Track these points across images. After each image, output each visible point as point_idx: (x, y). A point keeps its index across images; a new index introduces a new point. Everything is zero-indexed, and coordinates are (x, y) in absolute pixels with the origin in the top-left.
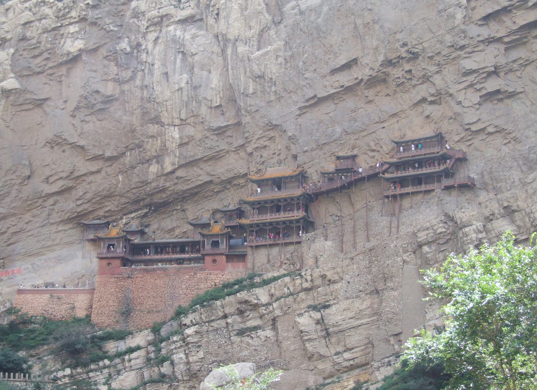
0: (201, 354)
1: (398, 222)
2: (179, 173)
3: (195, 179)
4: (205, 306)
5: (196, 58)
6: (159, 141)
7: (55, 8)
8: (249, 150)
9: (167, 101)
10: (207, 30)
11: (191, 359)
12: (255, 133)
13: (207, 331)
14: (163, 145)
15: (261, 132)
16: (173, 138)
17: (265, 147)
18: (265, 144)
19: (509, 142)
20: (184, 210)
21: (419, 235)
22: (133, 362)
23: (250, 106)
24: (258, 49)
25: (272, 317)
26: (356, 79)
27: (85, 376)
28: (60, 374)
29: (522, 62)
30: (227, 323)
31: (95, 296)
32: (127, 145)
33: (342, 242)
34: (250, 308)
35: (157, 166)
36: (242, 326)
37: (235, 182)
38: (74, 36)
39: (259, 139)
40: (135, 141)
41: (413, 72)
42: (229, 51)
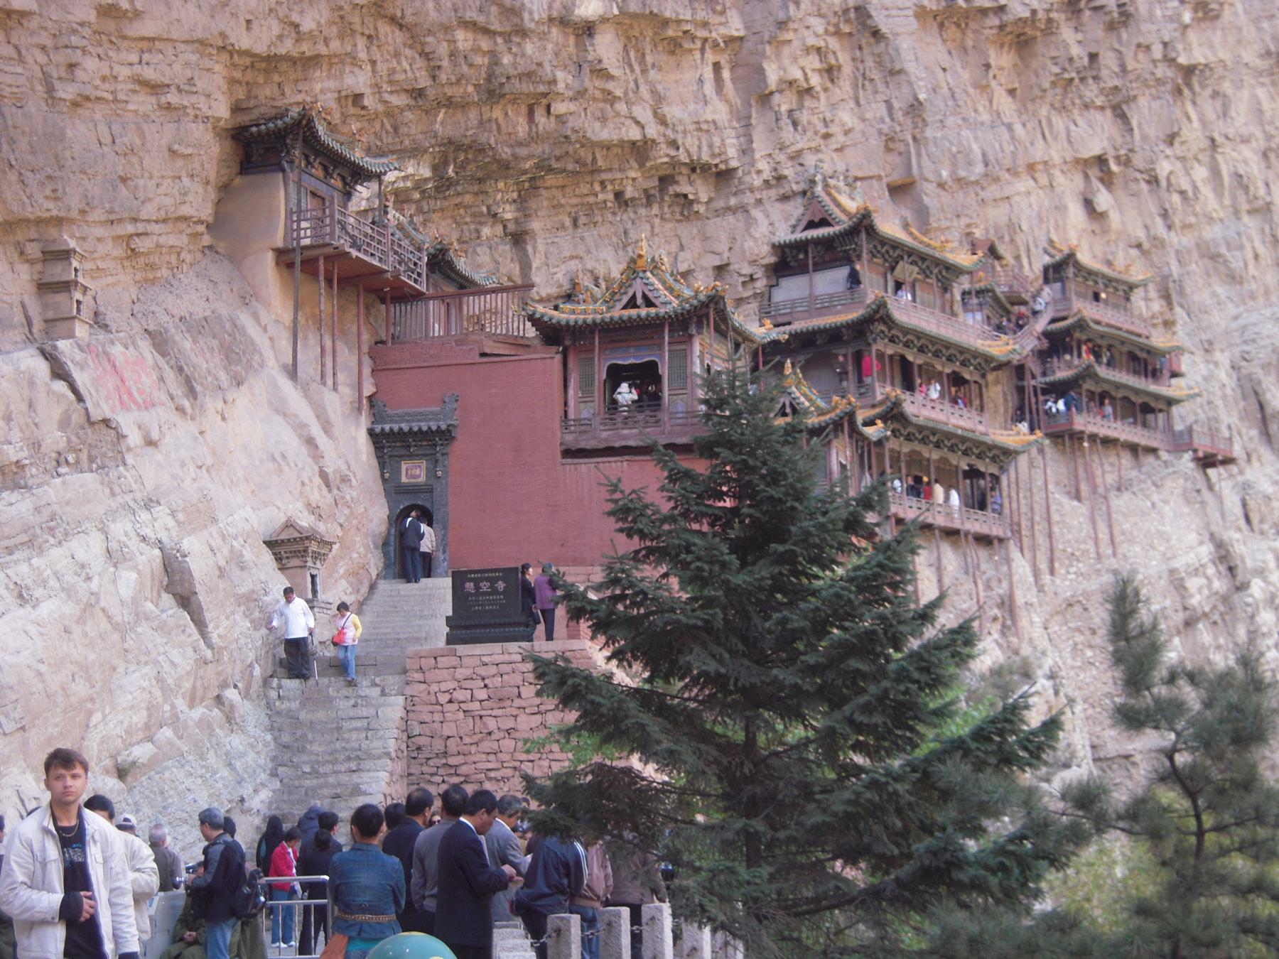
21: (1193, 584)
37: (685, 188)
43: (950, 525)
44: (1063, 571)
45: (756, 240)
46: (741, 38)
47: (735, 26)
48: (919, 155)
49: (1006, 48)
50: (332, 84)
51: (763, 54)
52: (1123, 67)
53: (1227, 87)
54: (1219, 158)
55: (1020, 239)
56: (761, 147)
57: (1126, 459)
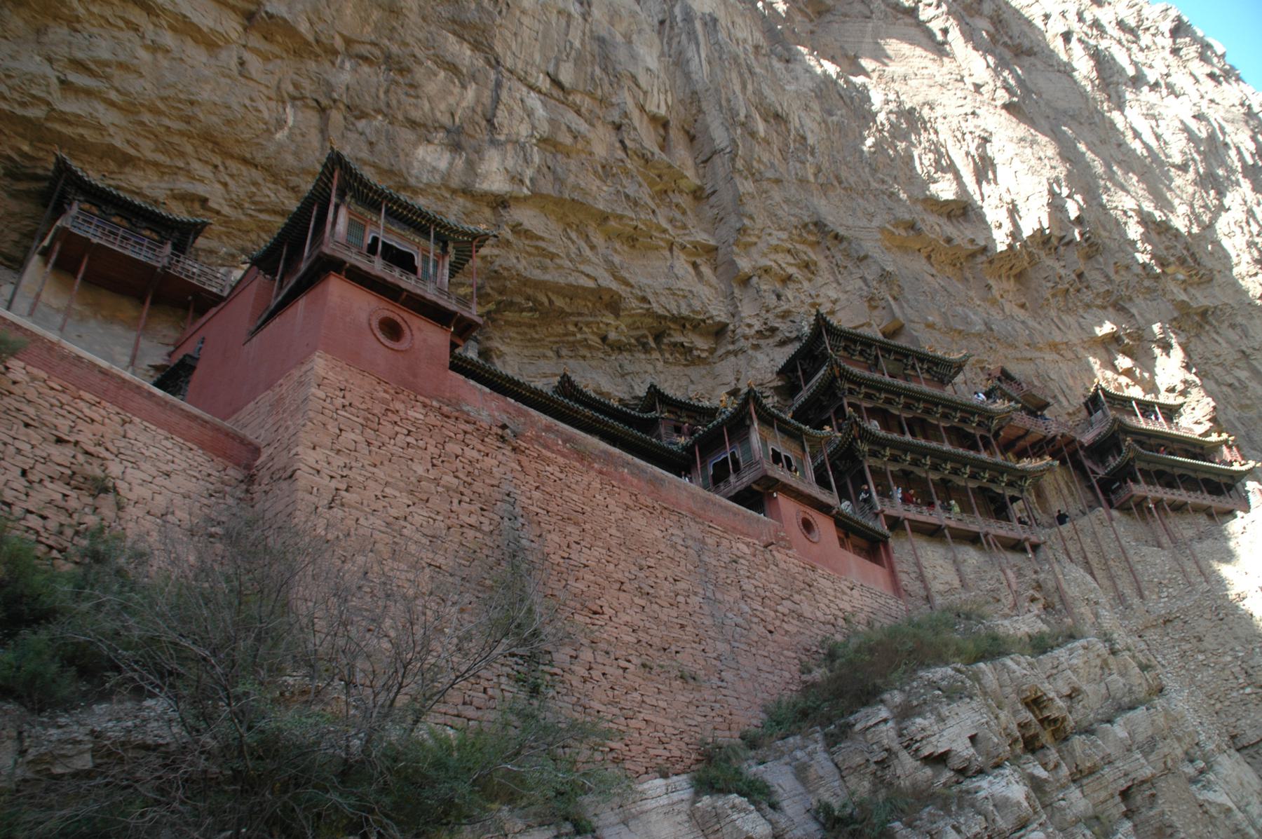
1: (1197, 563)
2: (527, 217)
3: (567, 264)
6: (471, 93)
9: (523, 12)
12: (769, 231)
14: (479, 110)
18: (791, 270)
23: (760, 161)
25: (1123, 784)
26: (972, 241)
32: (354, 37)
35: (447, 156)
37: (678, 338)
39: (776, 249)
40: (386, 42)
43: (961, 526)
44: (1154, 597)
45: (758, 370)
46: (716, 249)
47: (702, 237)
48: (901, 307)
49: (1004, 279)
50: (163, 185)
51: (732, 251)
52: (1107, 277)
53: (1239, 319)
54: (1255, 363)
55: (1051, 385)
56: (747, 310)
57: (1202, 520)
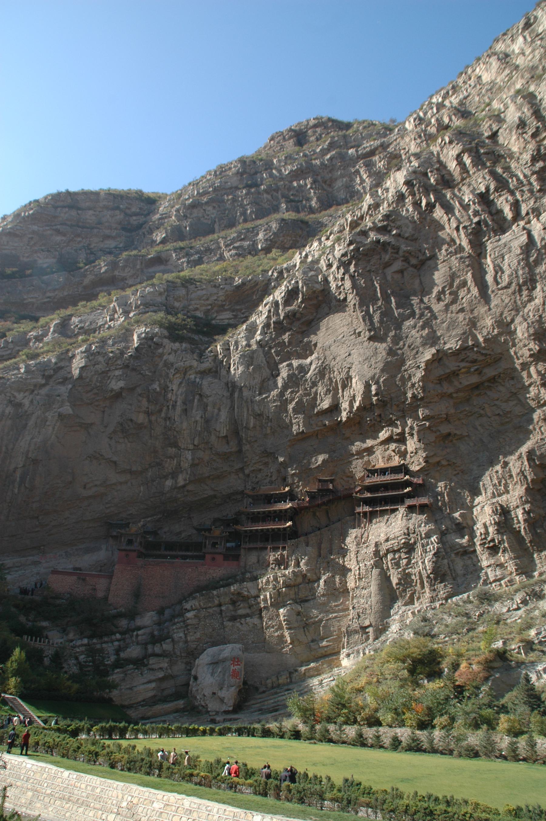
0: (198, 635)
2: (190, 488)
4: (202, 595)
5: (211, 399)
6: (175, 461)
7: (106, 357)
8: (247, 472)
10: (220, 379)
11: (189, 638)
13: (204, 616)
15: (257, 458)
16: (187, 459)
17: (260, 470)
18: (260, 467)
19: (458, 474)
20: (190, 518)
22: (140, 638)
23: (250, 437)
24: (260, 394)
27: (98, 646)
28: (79, 643)
29: (466, 413)
30: (221, 610)
31: (113, 580)
33: (320, 549)
34: (241, 599)
36: (233, 613)
38: (119, 378)
39: (255, 463)
41: (382, 415)
42: (236, 395)
54: (519, 396)
